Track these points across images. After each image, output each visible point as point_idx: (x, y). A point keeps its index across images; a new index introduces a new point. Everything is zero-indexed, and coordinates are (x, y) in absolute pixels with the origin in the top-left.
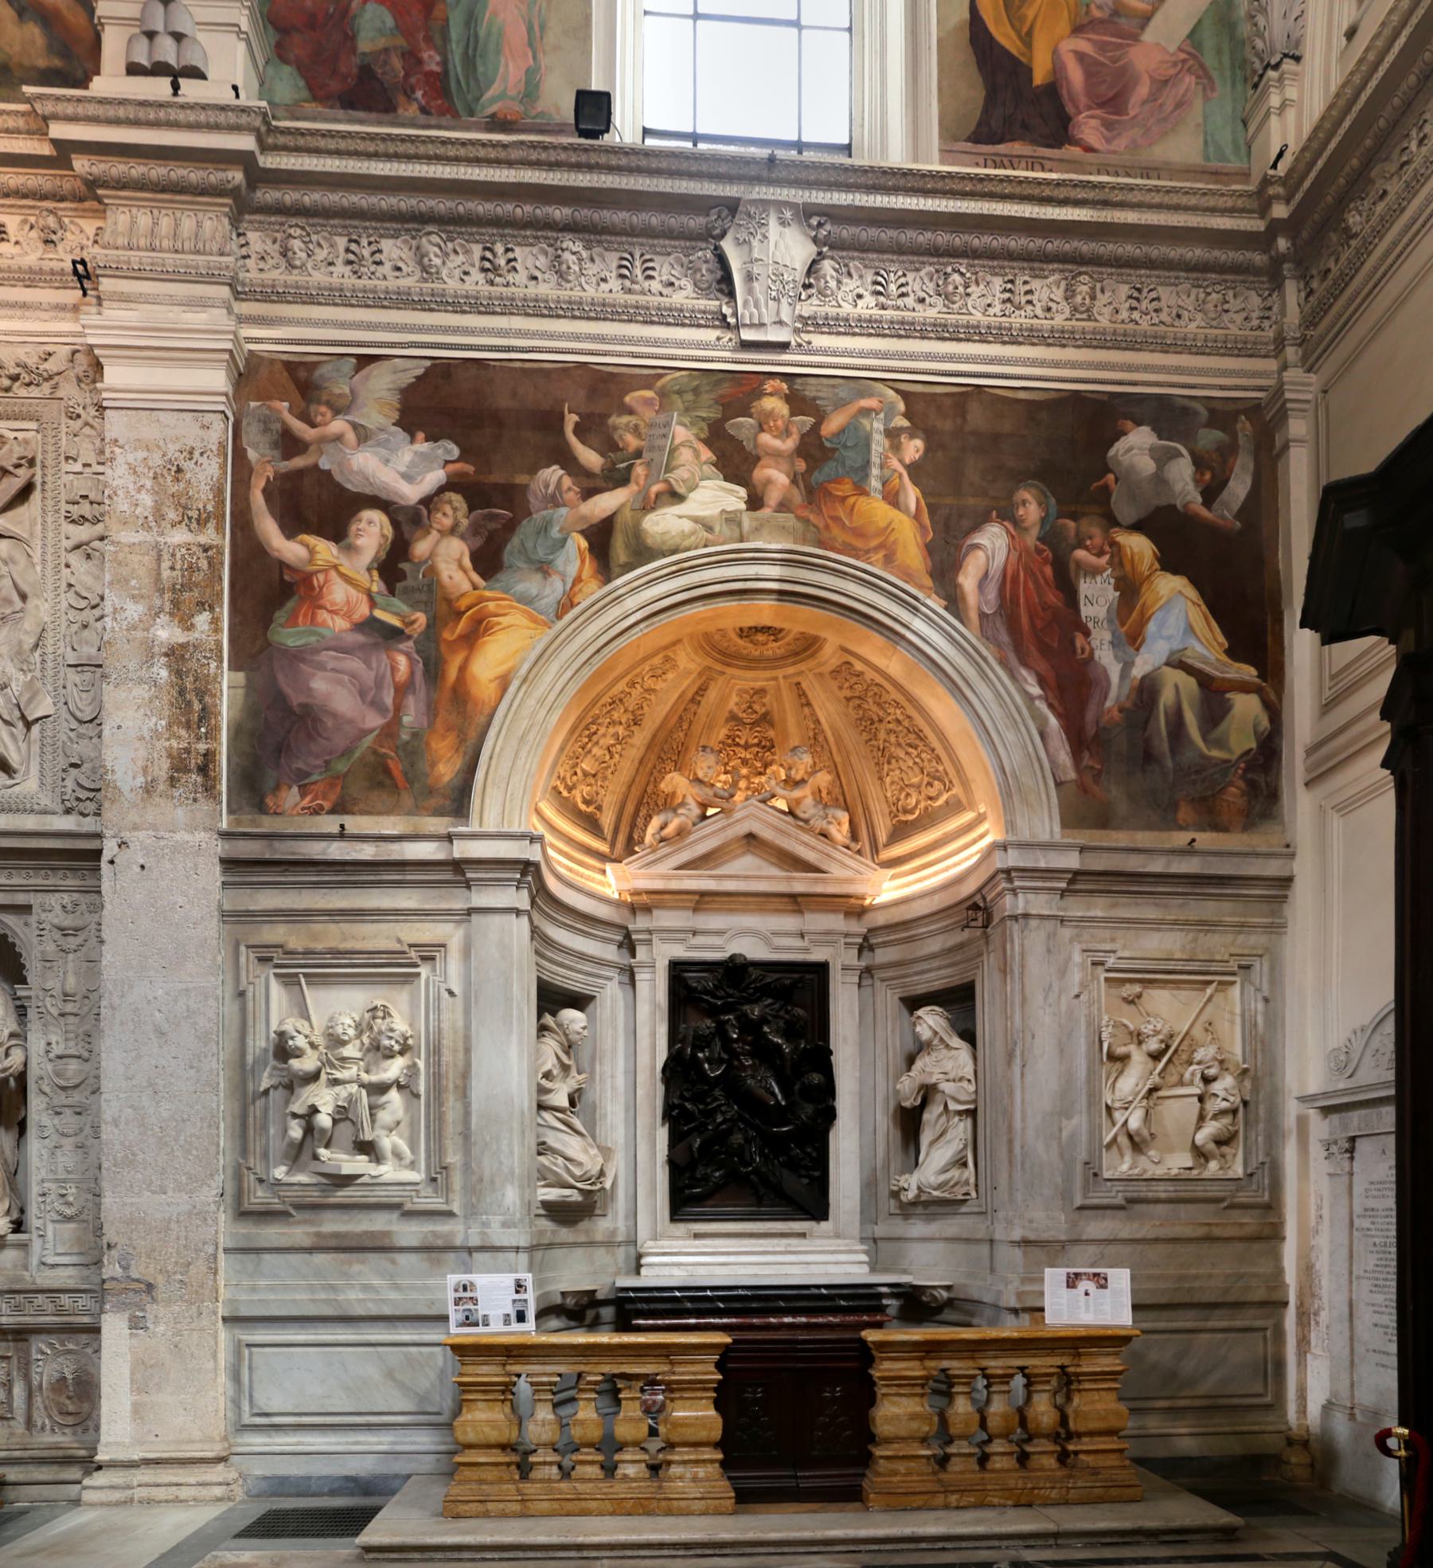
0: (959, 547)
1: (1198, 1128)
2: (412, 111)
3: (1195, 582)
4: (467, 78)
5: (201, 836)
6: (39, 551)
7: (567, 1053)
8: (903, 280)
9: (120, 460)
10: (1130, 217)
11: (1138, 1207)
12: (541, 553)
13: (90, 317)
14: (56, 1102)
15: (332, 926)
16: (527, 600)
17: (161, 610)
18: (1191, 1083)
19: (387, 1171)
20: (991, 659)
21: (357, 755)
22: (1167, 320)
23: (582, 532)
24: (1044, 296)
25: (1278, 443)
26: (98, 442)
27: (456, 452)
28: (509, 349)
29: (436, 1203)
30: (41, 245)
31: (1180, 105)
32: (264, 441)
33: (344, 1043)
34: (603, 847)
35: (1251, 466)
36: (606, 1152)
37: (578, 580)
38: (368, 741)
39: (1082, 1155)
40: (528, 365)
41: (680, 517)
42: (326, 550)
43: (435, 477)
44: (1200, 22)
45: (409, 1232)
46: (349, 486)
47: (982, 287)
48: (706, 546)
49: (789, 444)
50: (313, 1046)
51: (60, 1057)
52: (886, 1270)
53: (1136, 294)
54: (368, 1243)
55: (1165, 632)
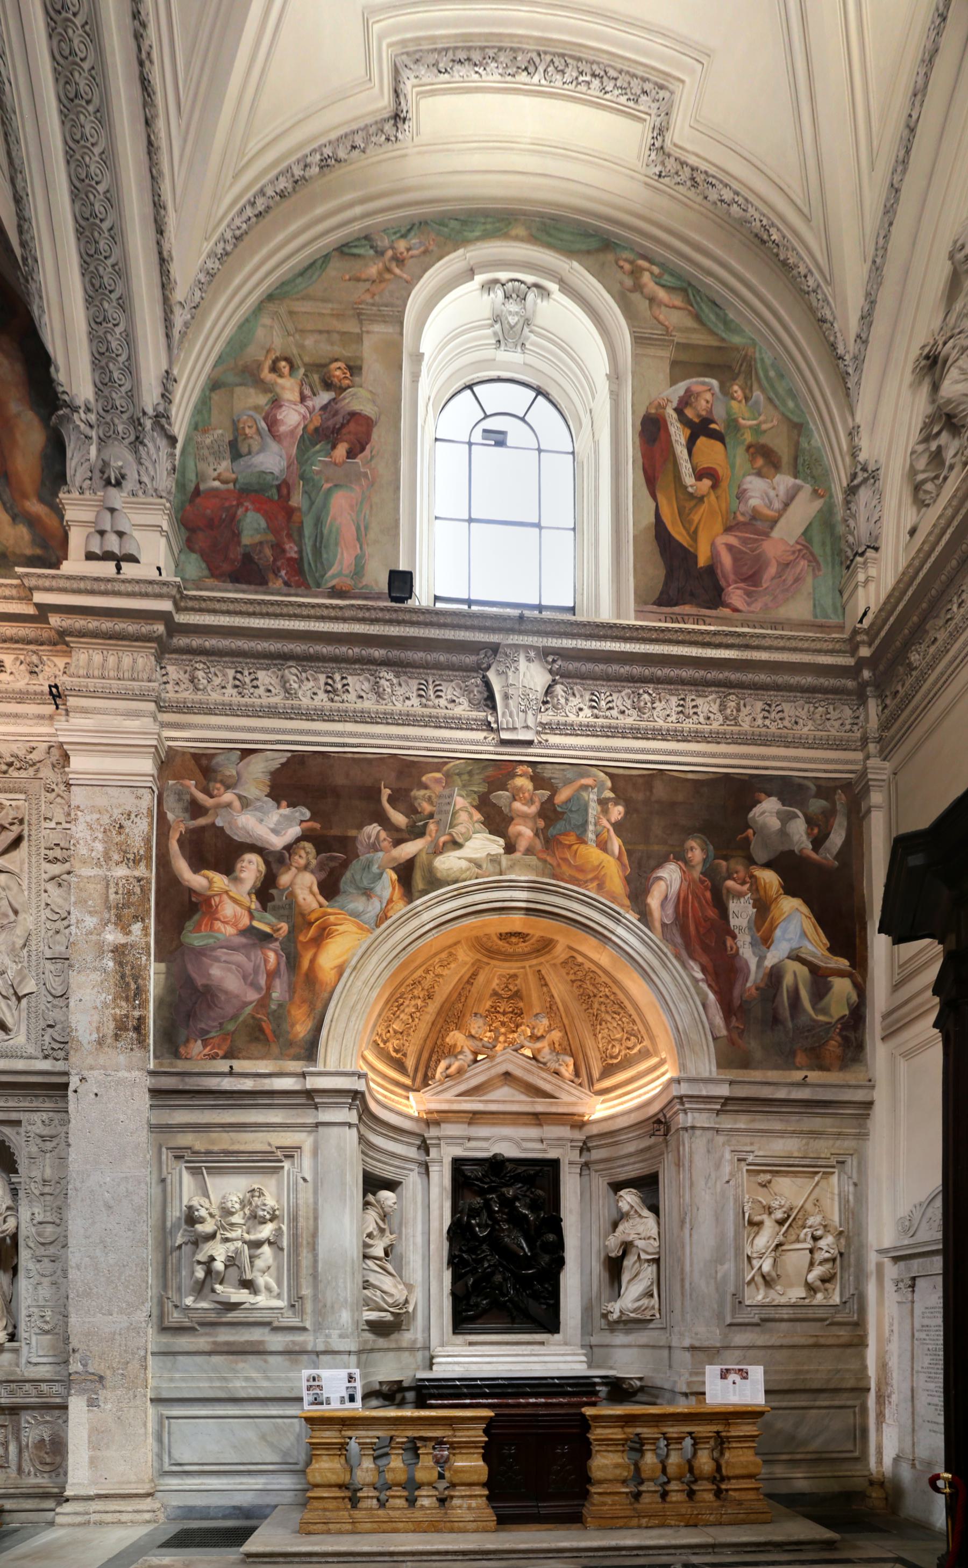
0: (648, 879)
1: (810, 1271)
2: (278, 584)
3: (807, 902)
4: (315, 562)
5: (136, 1073)
6: (26, 882)
7: (383, 1220)
9: (81, 819)
10: (764, 656)
11: (769, 1325)
12: (365, 883)
13: (61, 723)
14: (38, 1253)
15: (225, 1135)
16: (356, 915)
17: (109, 921)
18: (805, 1241)
19: (262, 1300)
20: (669, 954)
21: (241, 1019)
22: (789, 725)
26: (66, 808)
27: (308, 814)
28: (344, 745)
29: (295, 1321)
30: (28, 675)
31: (797, 580)
32: (178, 807)
33: (232, 1214)
34: (408, 1082)
36: (409, 1287)
37: (390, 901)
38: (248, 1010)
39: (731, 1289)
40: (356, 756)
42: (220, 881)
44: (810, 524)
45: (276, 1341)
46: (236, 838)
50: (211, 1215)
51: (40, 1223)
52: (599, 1367)
54: (248, 1349)
55: (787, 936)
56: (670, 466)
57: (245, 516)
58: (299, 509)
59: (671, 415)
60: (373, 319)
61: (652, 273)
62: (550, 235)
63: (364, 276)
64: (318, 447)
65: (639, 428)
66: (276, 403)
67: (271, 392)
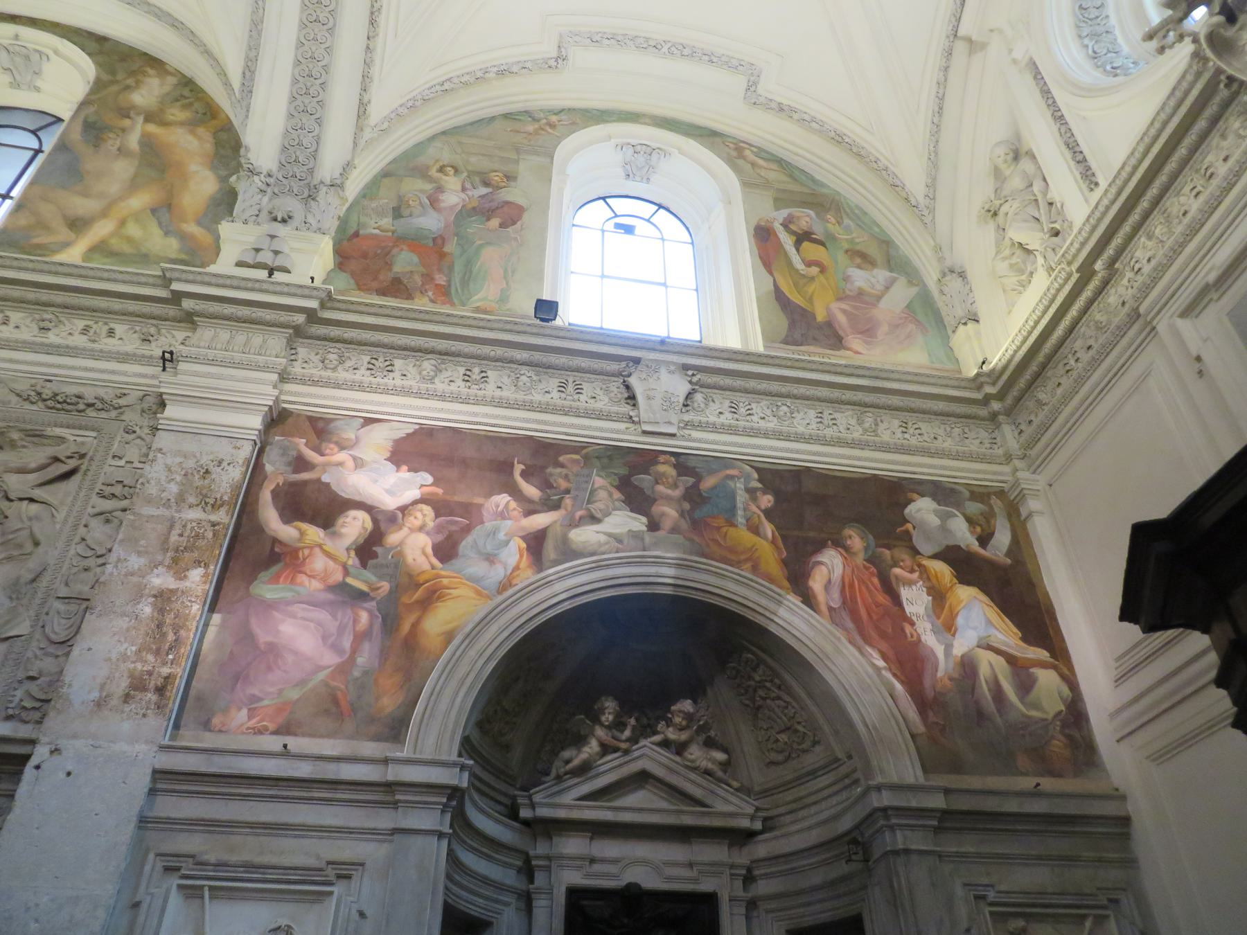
8: (749, 407)
12: (489, 548)
13: (165, 377)
15: (250, 838)
22: (928, 440)
23: (520, 537)
24: (844, 421)
25: (1024, 513)
26: (144, 450)
35: (1009, 526)
37: (517, 568)
41: (598, 532)
42: (314, 533)
43: (414, 494)
47: (802, 414)
48: (617, 552)
49: (677, 493)
53: (904, 425)
63: (522, 131)
64: (474, 218)
66: (440, 189)
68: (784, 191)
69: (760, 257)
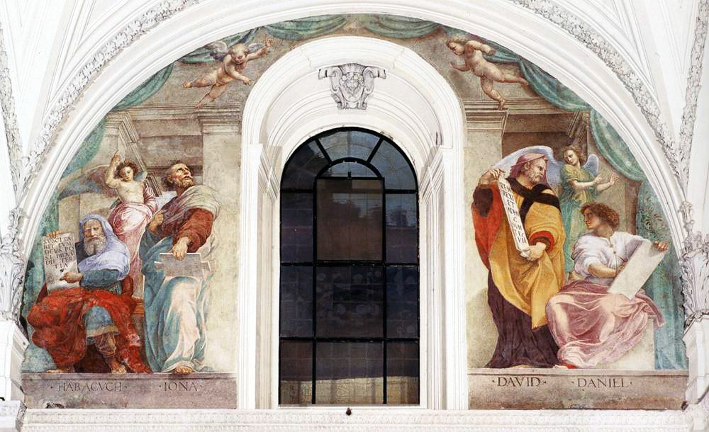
4: (156, 348)
31: (637, 333)
56: (503, 234)
57: (90, 310)
58: (142, 301)
59: (504, 184)
60: (213, 121)
61: (483, 52)
62: (383, 26)
63: (204, 82)
65: (471, 200)
66: (121, 204)
67: (115, 195)
68: (518, 118)
69: (477, 240)
